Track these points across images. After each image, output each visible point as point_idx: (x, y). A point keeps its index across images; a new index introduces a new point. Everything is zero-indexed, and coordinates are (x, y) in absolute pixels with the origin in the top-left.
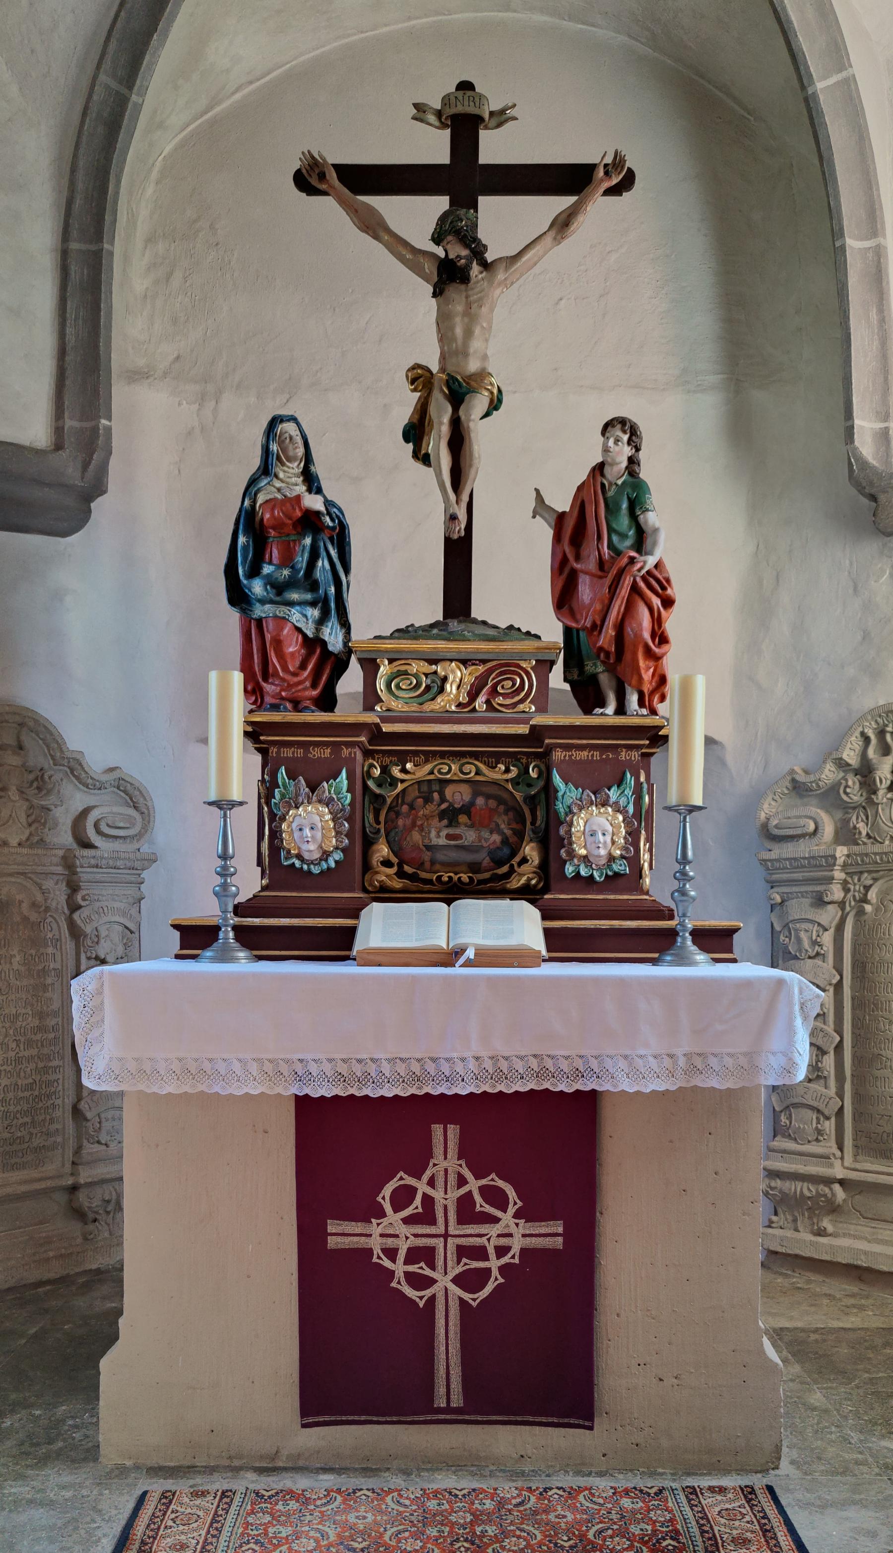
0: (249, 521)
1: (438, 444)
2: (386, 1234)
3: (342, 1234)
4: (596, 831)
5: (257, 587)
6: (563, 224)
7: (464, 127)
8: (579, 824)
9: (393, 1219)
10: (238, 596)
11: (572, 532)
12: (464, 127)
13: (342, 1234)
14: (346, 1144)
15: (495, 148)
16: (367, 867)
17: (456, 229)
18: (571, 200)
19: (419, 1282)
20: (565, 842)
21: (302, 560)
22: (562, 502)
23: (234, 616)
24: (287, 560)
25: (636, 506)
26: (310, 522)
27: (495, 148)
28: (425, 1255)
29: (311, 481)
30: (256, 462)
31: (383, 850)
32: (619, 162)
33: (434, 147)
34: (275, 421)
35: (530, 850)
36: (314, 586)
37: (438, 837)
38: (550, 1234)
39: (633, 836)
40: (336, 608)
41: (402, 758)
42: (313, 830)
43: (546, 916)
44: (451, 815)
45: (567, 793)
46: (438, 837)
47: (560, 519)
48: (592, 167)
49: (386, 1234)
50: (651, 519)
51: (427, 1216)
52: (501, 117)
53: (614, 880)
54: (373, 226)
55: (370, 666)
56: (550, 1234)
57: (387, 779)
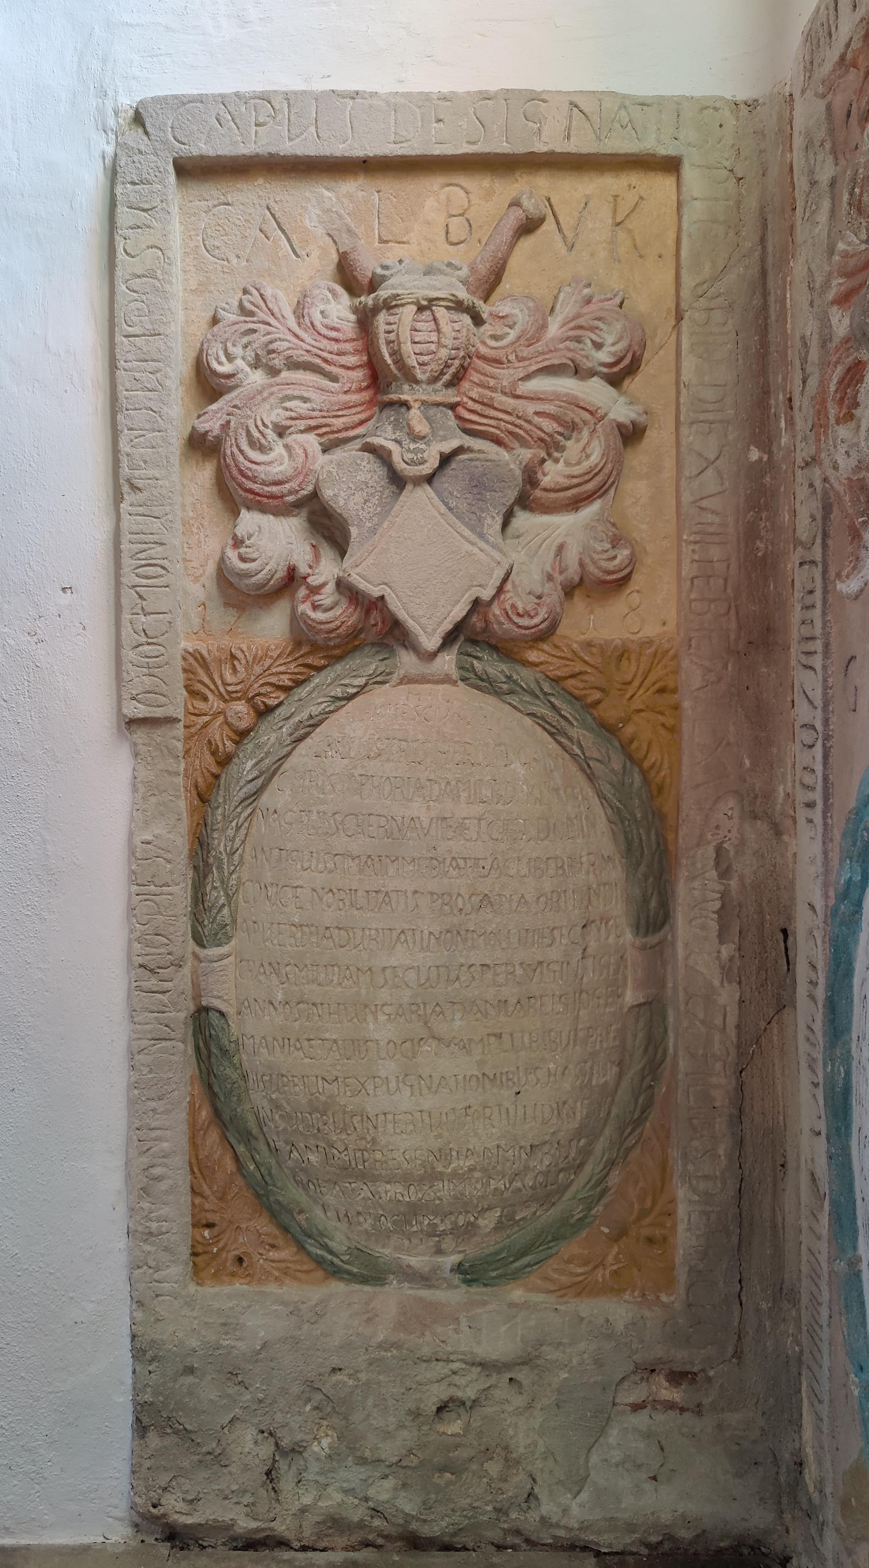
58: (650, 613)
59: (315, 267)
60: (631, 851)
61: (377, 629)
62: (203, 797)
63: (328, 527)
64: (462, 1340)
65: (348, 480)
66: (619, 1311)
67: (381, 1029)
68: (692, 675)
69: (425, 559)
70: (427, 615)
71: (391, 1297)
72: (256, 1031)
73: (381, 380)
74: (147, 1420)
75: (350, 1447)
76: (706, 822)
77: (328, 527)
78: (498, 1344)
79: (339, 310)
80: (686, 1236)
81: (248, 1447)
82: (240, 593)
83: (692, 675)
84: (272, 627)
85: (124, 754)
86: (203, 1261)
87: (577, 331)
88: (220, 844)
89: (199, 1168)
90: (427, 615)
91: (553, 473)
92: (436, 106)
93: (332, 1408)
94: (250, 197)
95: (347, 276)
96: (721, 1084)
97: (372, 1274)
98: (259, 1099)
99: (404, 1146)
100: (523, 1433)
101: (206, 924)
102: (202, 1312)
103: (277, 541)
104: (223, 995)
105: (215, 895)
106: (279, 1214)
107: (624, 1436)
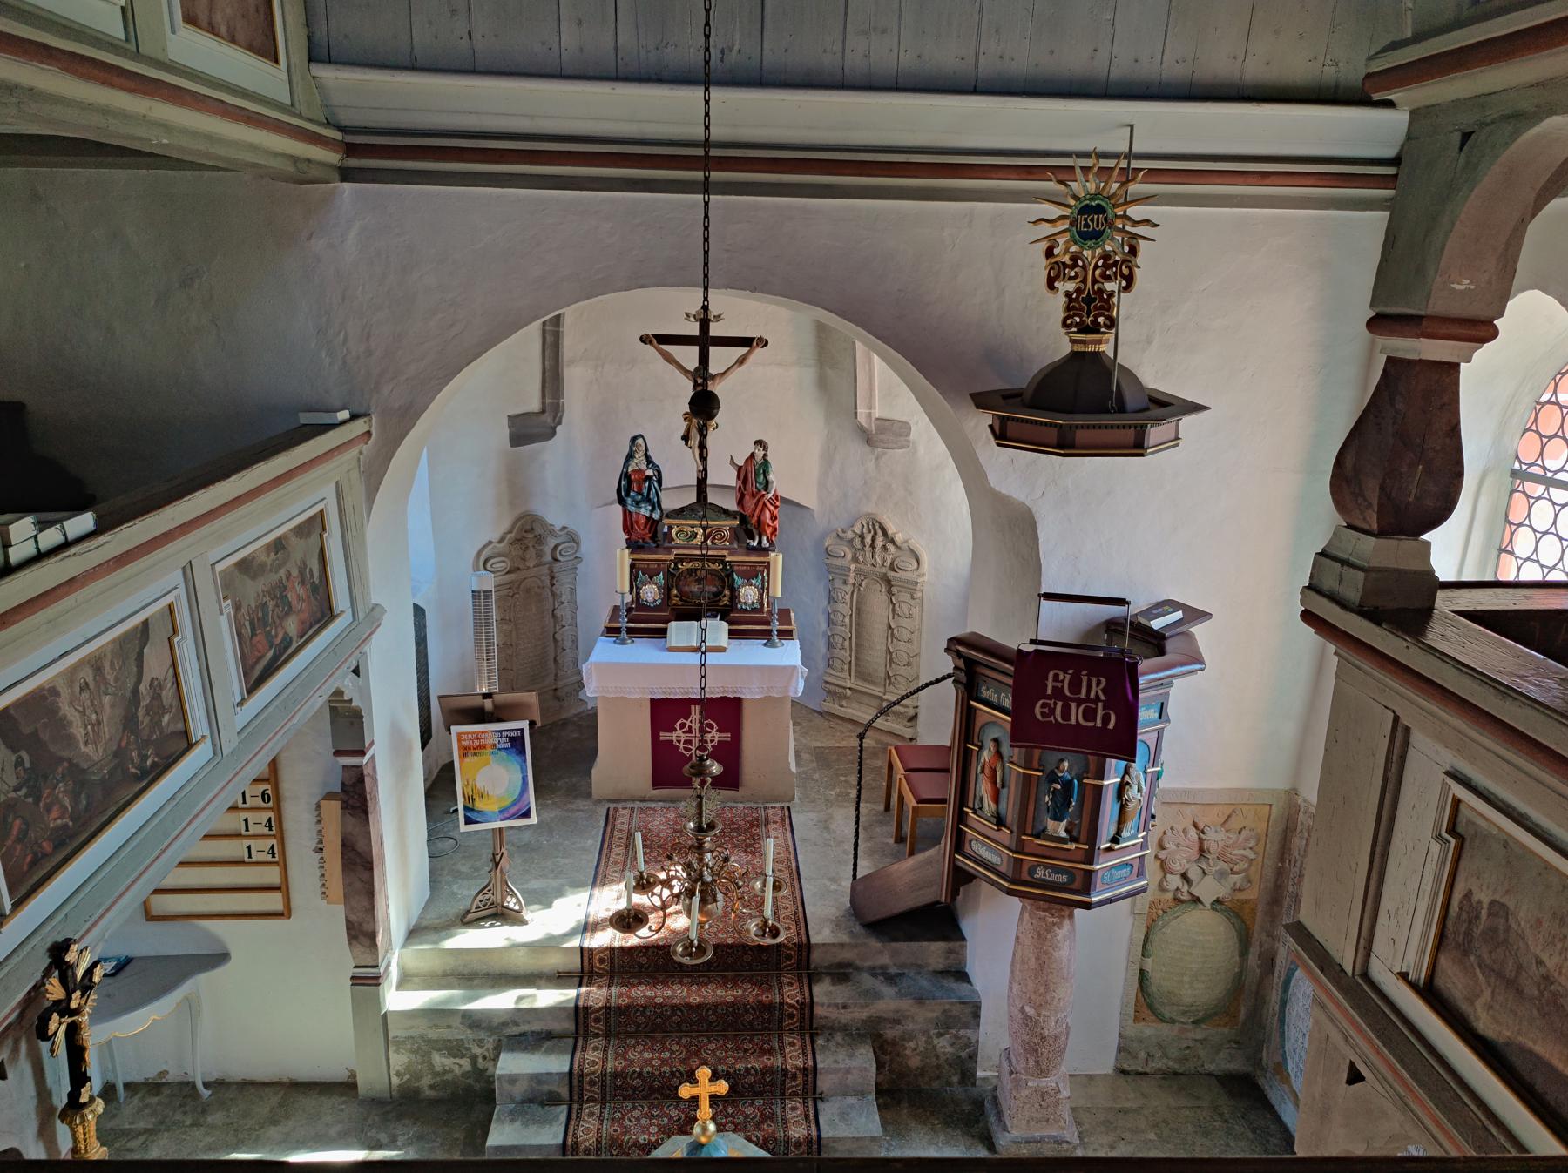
0: (626, 476)
1: (695, 439)
2: (677, 736)
3: (664, 736)
4: (748, 594)
5: (629, 501)
6: (741, 361)
7: (704, 324)
8: (742, 591)
9: (680, 732)
10: (621, 501)
11: (743, 474)
12: (704, 324)
13: (664, 736)
14: (665, 712)
15: (715, 330)
16: (669, 598)
17: (704, 359)
18: (746, 350)
19: (687, 749)
20: (738, 597)
21: (645, 492)
22: (741, 463)
23: (620, 508)
24: (640, 493)
25: (765, 473)
26: (649, 478)
27: (715, 330)
28: (690, 742)
29: (649, 461)
30: (627, 450)
31: (675, 592)
32: (760, 339)
33: (693, 329)
34: (634, 439)
35: (727, 592)
36: (648, 500)
37: (695, 588)
38: (727, 737)
39: (761, 595)
40: (657, 505)
41: (681, 561)
42: (650, 593)
43: (730, 623)
44: (699, 581)
45: (738, 580)
46: (695, 588)
47: (740, 468)
48: (752, 339)
49: (677, 736)
50: (771, 477)
51: (690, 731)
52: (718, 318)
53: (754, 610)
54: (669, 359)
55: (671, 528)
56: (727, 737)
57: (676, 568)
58: (1252, 894)
59: (1188, 824)
60: (1240, 940)
61: (1196, 900)
62: (1149, 929)
63: (1184, 876)
64: (1191, 1035)
65: (1194, 874)
66: (1226, 1030)
67: (1186, 979)
68: (1260, 908)
69: (1209, 889)
70: (1208, 899)
71: (1177, 1026)
72: (1157, 977)
73: (1202, 851)
74: (1120, 1050)
75: (1165, 1055)
76: (1258, 936)
77: (1184, 876)
78: (1199, 1037)
79: (1193, 834)
80: (1242, 1017)
81: (1143, 1055)
82: (1161, 888)
83: (1260, 908)
84: (1169, 896)
85: (1131, 920)
86: (1136, 1019)
87: (1246, 840)
88: (1151, 938)
89: (1137, 1001)
90: (1208, 899)
91: (1236, 868)
92: (1219, 791)
93: (1160, 1046)
94: (1175, 808)
95: (1195, 825)
96: (1254, 988)
97: (1173, 1021)
98: (1154, 988)
99: (1188, 1000)
100: (1202, 1053)
101: (1145, 953)
102: (1133, 1030)
103: (1174, 881)
104: (1149, 965)
105: (1149, 947)
106: (1151, 1007)
107: (1223, 1054)
